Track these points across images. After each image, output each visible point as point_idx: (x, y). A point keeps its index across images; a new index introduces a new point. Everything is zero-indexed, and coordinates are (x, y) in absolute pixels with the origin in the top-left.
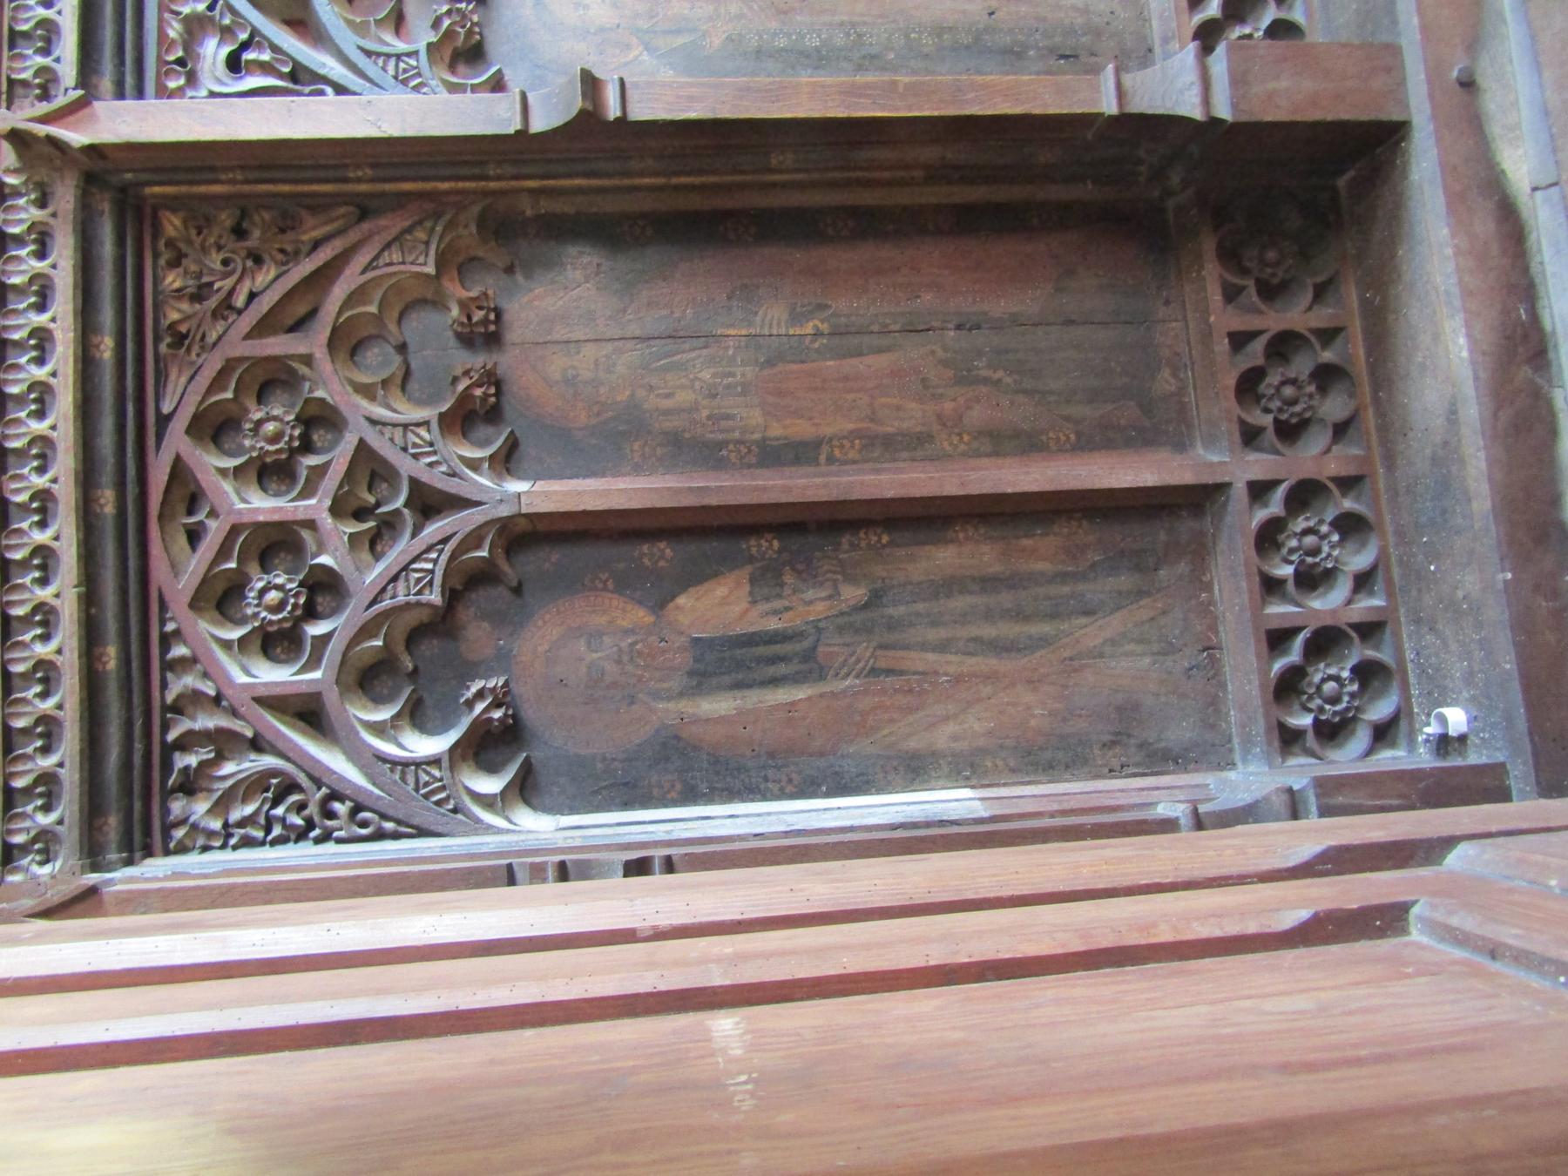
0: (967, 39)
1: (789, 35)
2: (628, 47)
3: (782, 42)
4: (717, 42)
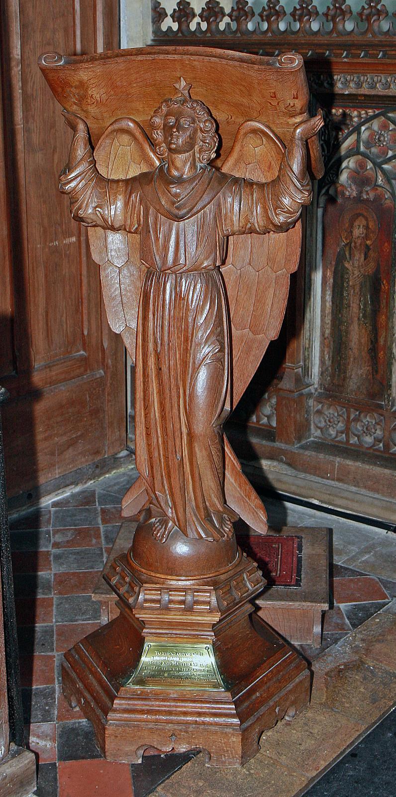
0: (344, 339)
1: (347, 287)
2: (346, 239)
3: (345, 285)
4: (347, 265)
